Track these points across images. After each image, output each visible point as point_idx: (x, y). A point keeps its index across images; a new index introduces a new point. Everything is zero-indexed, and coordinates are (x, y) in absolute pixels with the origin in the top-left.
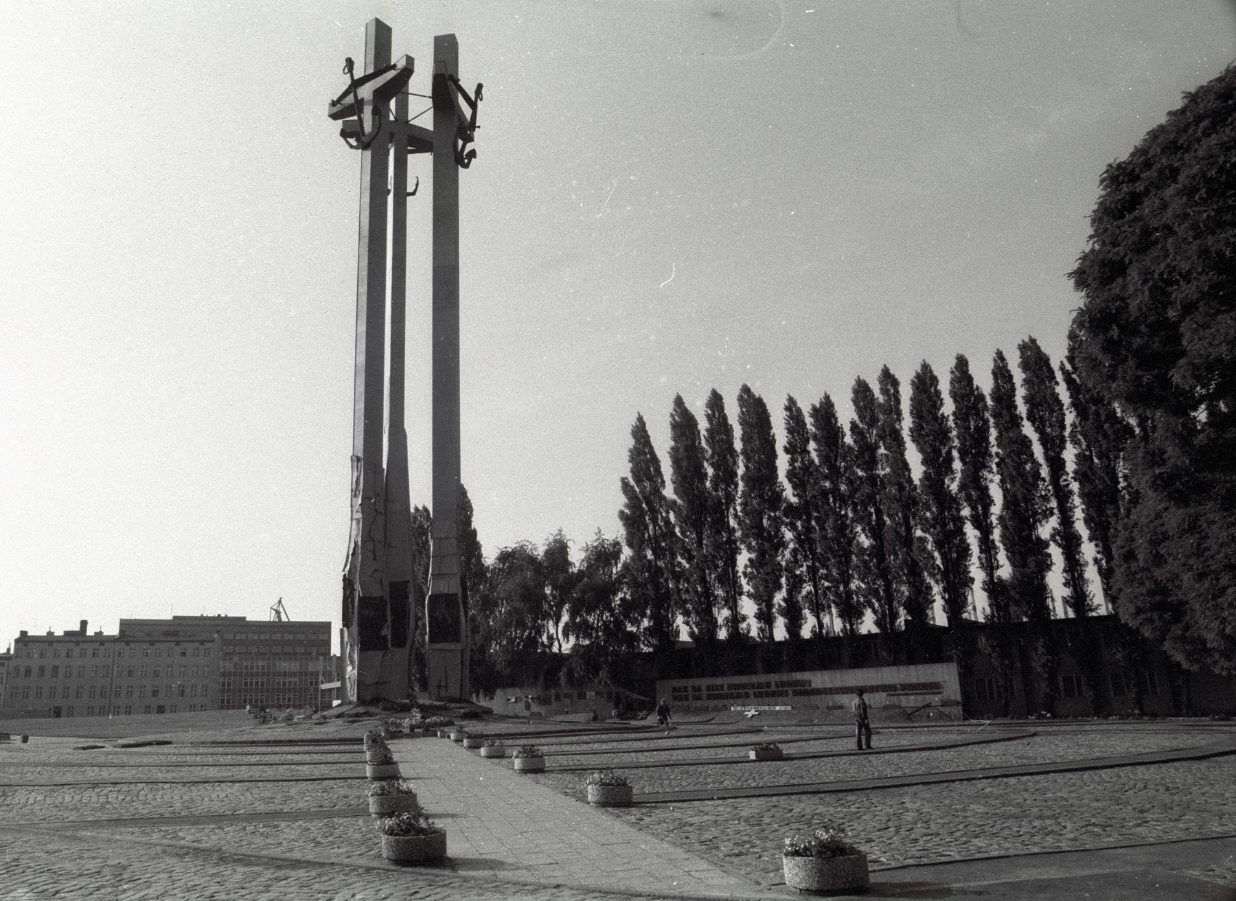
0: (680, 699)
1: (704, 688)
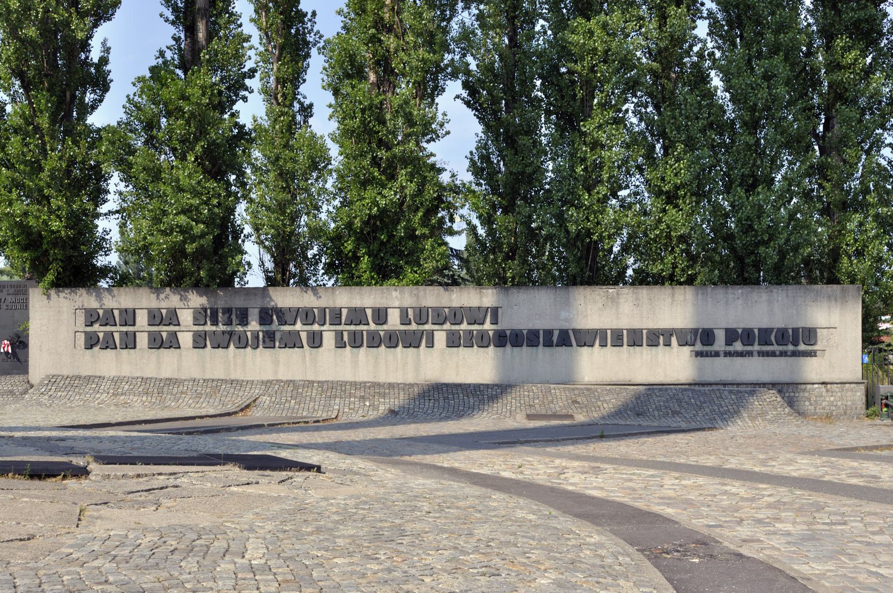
0: (109, 344)
1: (186, 317)
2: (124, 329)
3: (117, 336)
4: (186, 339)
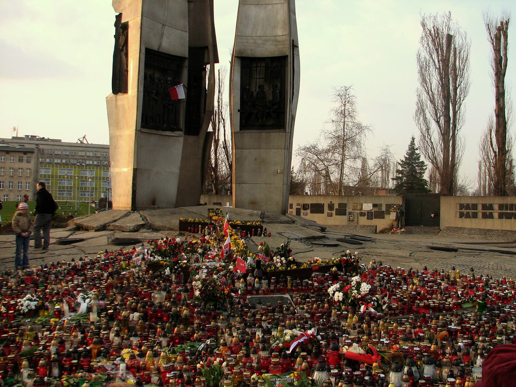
0: (468, 216)
1: (496, 207)
2: (473, 211)
3: (471, 213)
4: (496, 215)
